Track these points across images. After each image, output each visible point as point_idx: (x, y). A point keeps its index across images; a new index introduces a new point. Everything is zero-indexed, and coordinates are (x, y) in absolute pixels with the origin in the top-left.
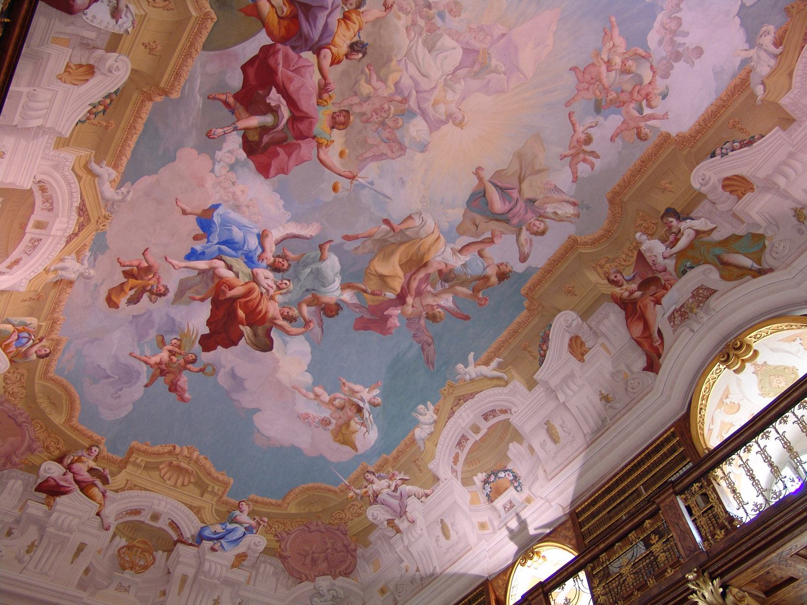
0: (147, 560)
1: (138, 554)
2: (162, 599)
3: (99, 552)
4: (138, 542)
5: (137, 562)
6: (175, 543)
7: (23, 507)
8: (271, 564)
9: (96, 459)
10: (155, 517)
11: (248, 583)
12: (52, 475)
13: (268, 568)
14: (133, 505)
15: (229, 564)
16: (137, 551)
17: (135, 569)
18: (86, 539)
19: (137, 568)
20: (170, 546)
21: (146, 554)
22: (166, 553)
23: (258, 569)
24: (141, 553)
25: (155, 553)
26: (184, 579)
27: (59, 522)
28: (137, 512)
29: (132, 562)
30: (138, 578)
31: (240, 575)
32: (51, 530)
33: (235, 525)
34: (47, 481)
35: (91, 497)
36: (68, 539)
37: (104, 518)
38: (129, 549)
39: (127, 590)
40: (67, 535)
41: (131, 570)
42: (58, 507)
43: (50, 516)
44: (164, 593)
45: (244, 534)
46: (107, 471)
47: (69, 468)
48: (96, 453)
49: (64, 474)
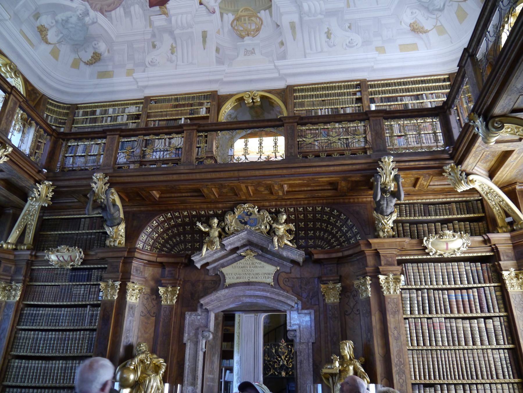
0: (256, 23)
1: (247, 21)
2: (283, 48)
3: (218, 32)
4: (242, 12)
5: (249, 28)
7: (151, 23)
11: (348, 6)
16: (245, 20)
17: (251, 34)
19: (252, 33)
21: (253, 19)
22: (267, 11)
24: (249, 20)
25: (259, 15)
26: (293, 26)
27: (180, 24)
29: (246, 30)
32: (177, 32)
37: (207, 5)
38: (238, 20)
39: (253, 52)
40: (190, 30)
41: (248, 36)
42: (172, 12)
43: (171, 21)
44: (282, 44)
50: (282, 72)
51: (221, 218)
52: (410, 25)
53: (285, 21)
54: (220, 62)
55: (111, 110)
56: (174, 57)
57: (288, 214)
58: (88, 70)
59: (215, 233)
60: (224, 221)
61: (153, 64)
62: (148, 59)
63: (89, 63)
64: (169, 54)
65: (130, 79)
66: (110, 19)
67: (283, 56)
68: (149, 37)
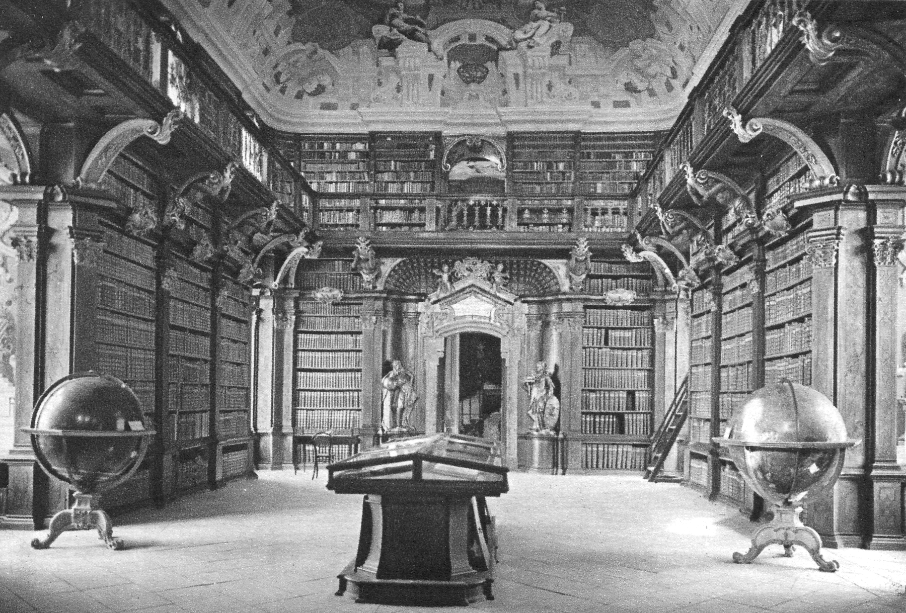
6: (497, 52)
8: (585, 43)
9: (405, 12)
10: (472, 37)
11: (570, 64)
12: (384, 34)
13: (583, 46)
14: (453, 34)
15: (548, 53)
18: (432, 71)
20: (494, 56)
23: (575, 50)
26: (516, 76)
28: (457, 39)
30: (481, 87)
31: (562, 60)
33: (539, 22)
34: (382, 39)
35: (420, 40)
36: (419, 75)
41: (474, 81)
42: (400, 55)
43: (398, 63)
44: (505, 92)
45: (550, 27)
46: (418, 17)
47: (391, 25)
48: (402, 7)
49: (391, 30)
50: (504, 118)
51: (451, 265)
52: (625, 84)
53: (510, 72)
54: (444, 104)
55: (338, 146)
56: (400, 95)
57: (504, 263)
58: (311, 100)
59: (445, 277)
60: (453, 266)
61: (377, 100)
62: (373, 96)
63: (312, 94)
64: (395, 92)
65: (354, 112)
66: (338, 56)
67: (506, 105)
68: (375, 74)
